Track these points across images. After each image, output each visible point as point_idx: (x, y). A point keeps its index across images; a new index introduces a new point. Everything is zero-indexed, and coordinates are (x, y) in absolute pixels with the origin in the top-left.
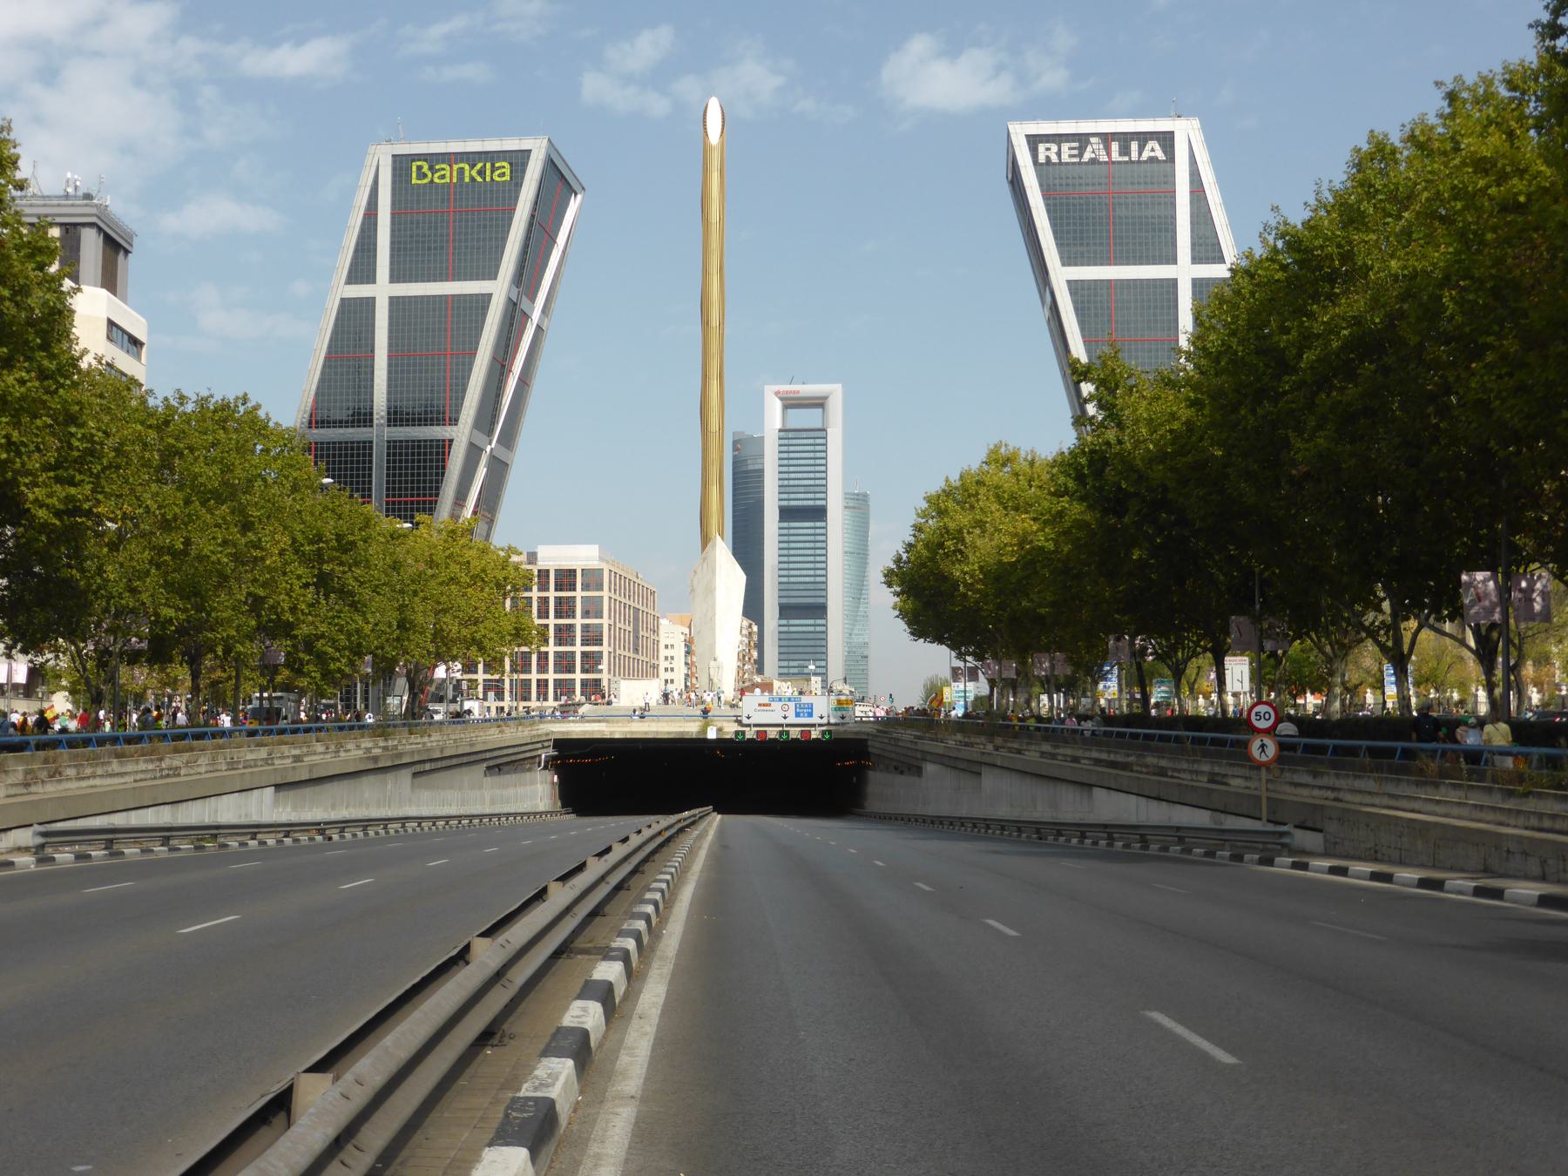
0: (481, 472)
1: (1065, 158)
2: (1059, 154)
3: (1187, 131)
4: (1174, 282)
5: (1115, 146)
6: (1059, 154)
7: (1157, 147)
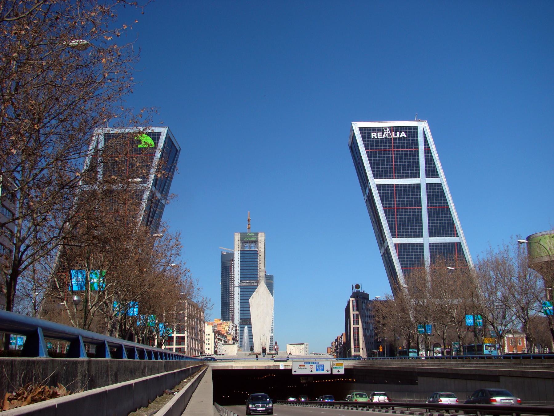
3: (422, 126)
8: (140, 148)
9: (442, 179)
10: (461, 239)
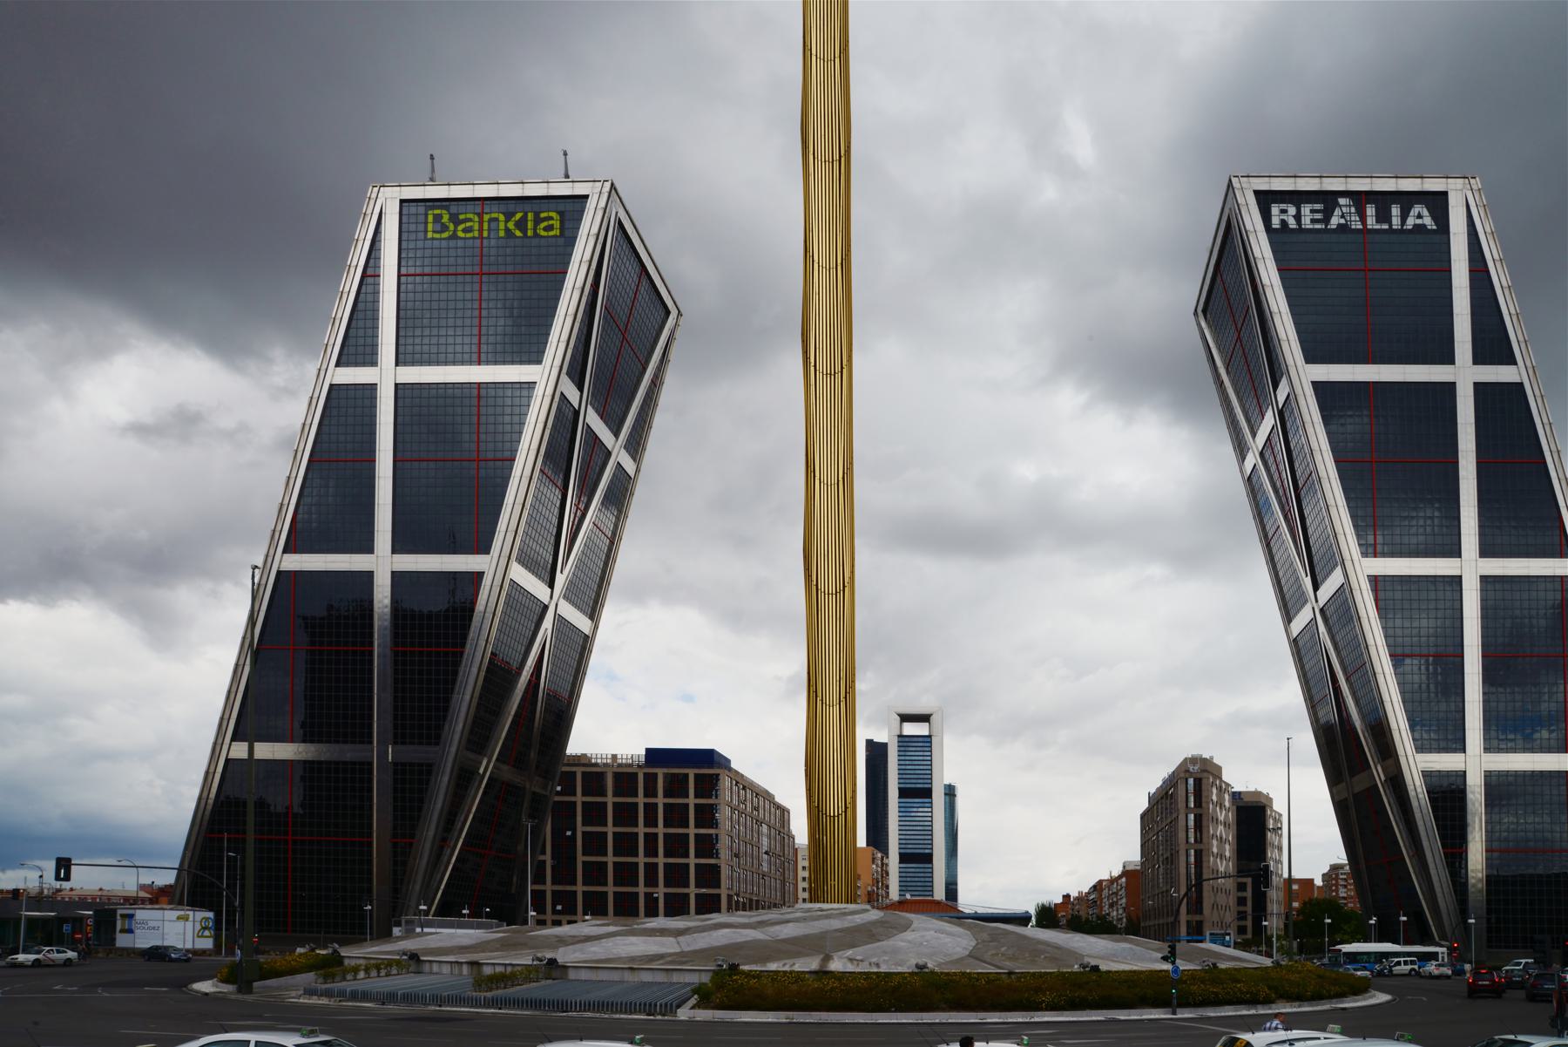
1: (1306, 222)
2: (1298, 217)
4: (1451, 387)
5: (1370, 211)
6: (1298, 217)
7: (1425, 212)
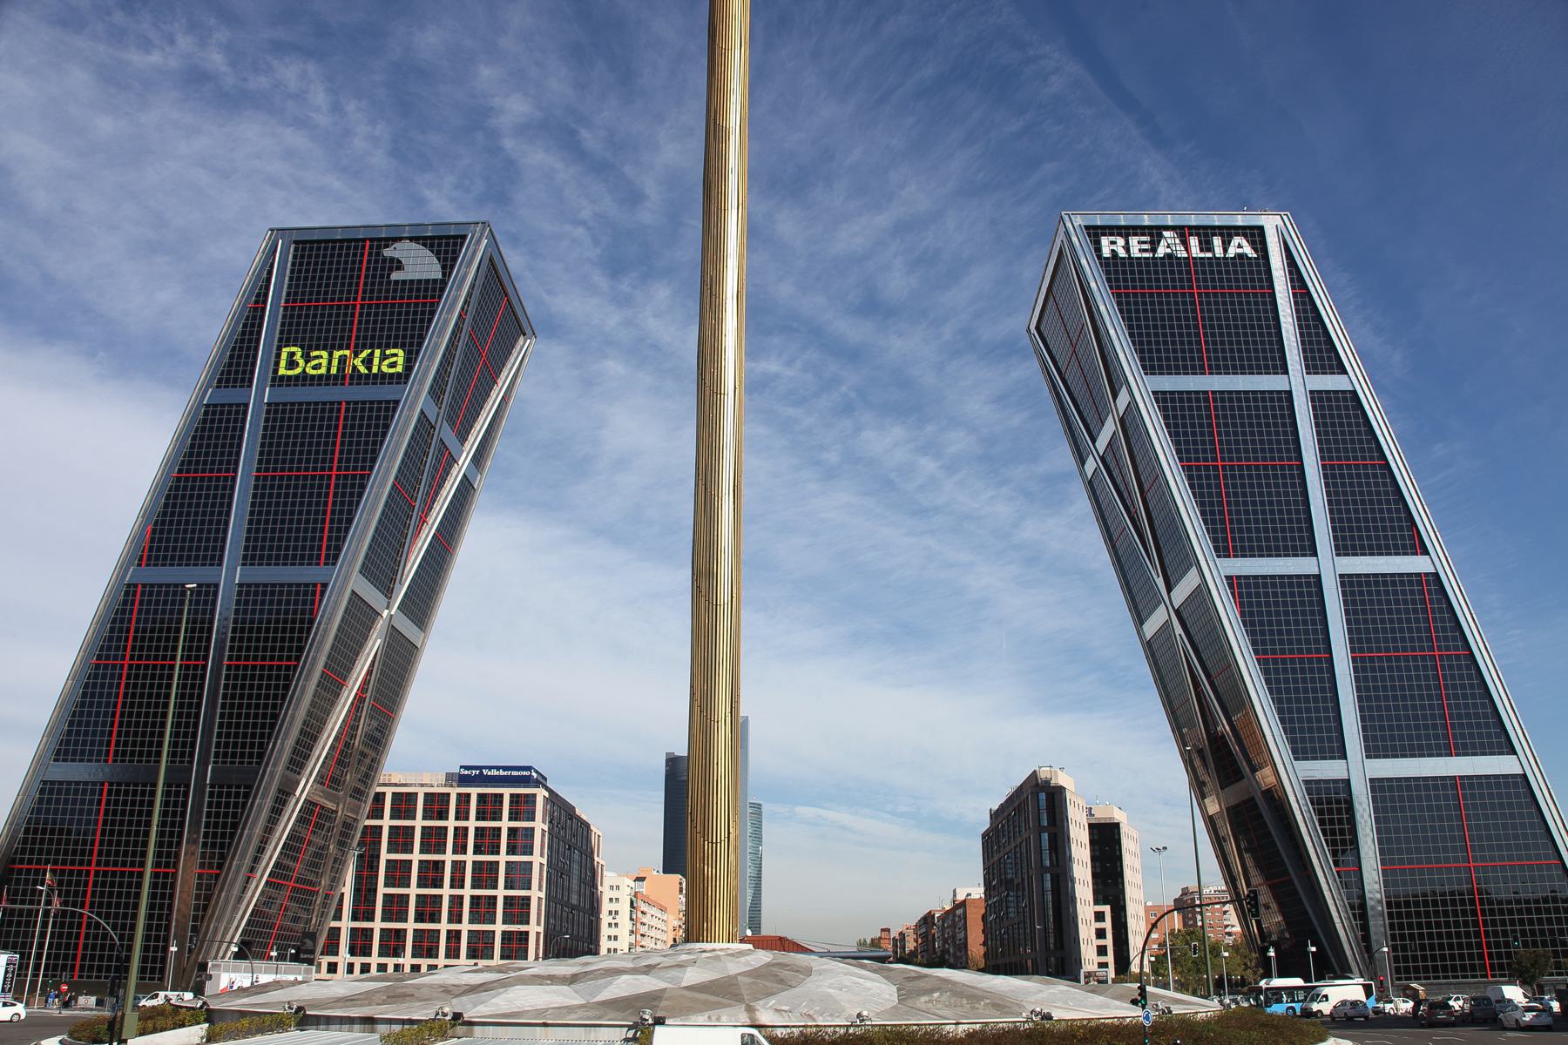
0: (375, 644)
1: (1135, 252)
2: (1127, 248)
5: (1194, 241)
6: (1127, 248)
7: (1244, 243)
8: (396, 282)
9: (1355, 378)
10: (1436, 559)
